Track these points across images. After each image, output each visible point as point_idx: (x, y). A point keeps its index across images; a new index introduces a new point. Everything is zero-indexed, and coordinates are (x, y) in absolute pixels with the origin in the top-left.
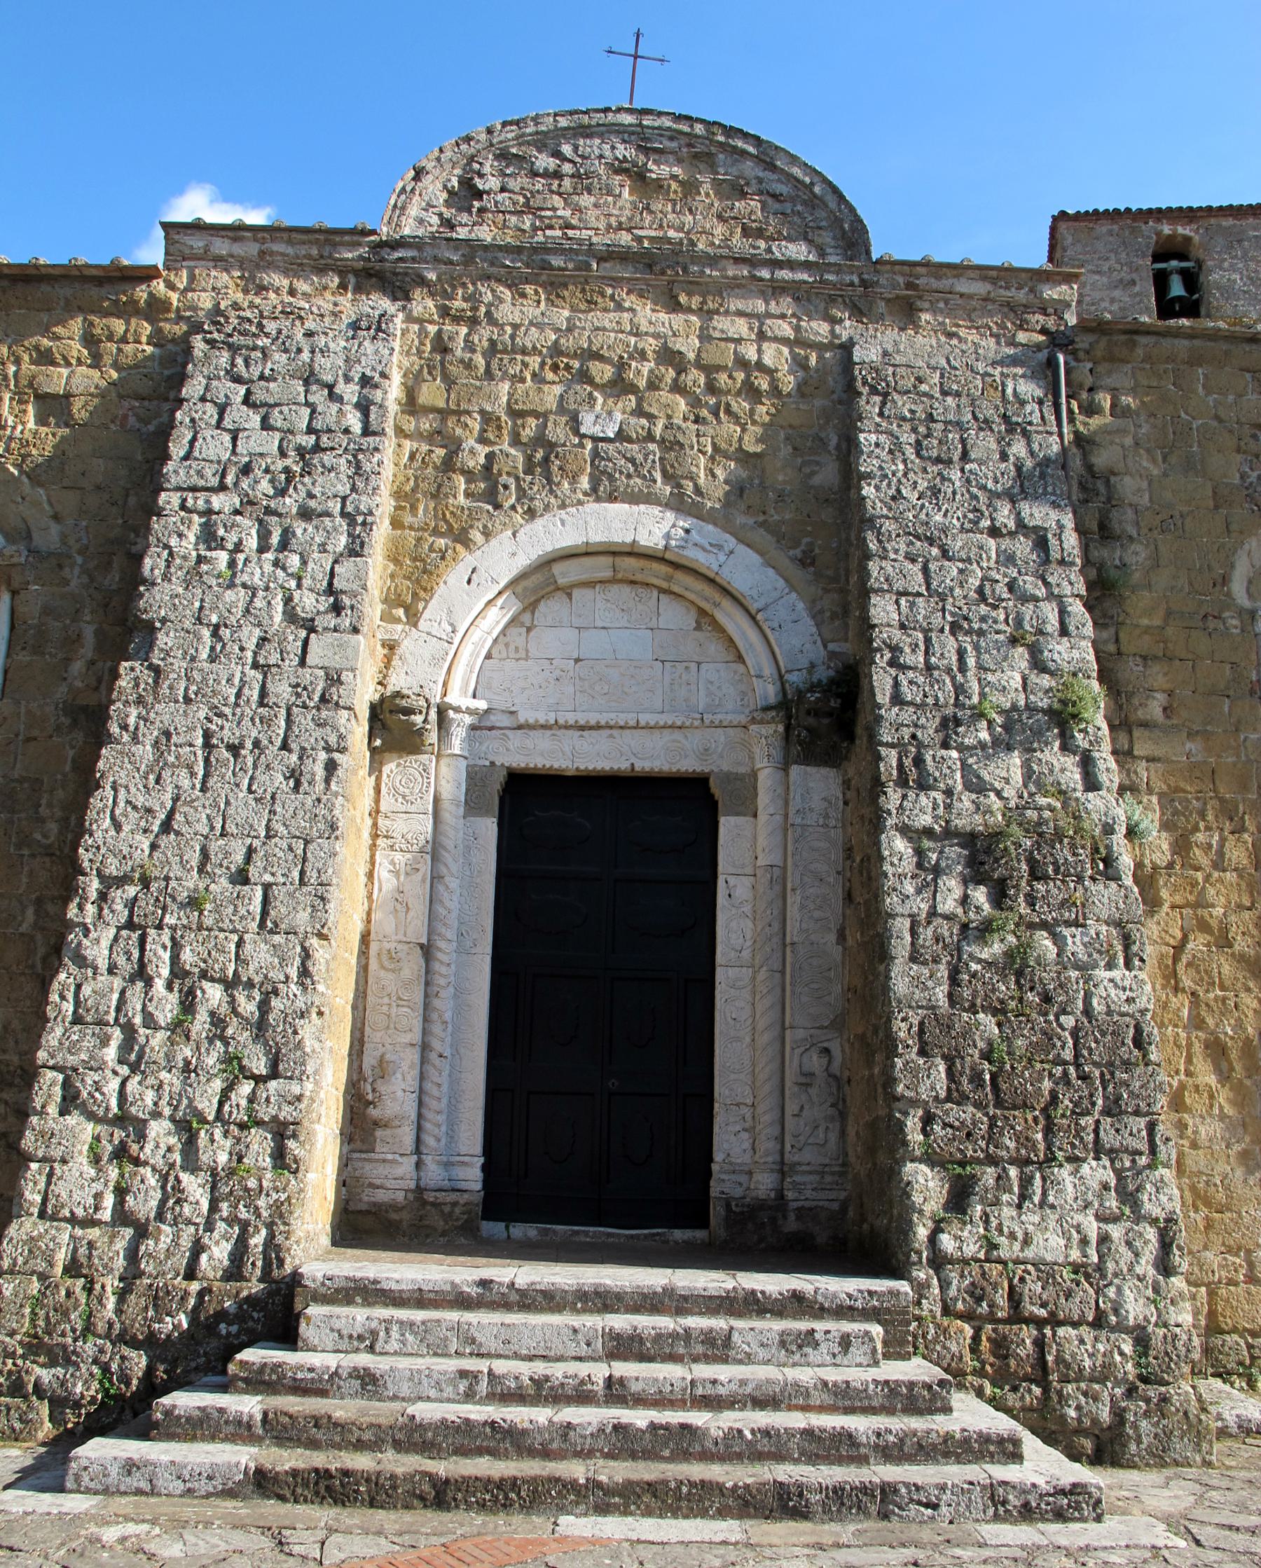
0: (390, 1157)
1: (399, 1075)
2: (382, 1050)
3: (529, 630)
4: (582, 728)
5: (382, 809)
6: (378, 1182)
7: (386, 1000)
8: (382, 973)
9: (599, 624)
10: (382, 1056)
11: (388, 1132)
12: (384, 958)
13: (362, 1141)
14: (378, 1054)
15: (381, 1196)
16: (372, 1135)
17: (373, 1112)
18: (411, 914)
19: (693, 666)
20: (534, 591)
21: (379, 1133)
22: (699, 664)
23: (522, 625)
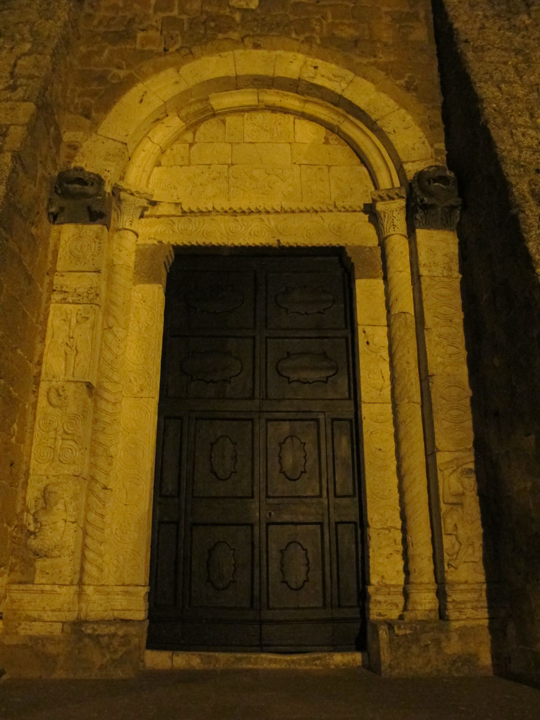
0: (48, 588)
1: (60, 506)
2: (46, 482)
3: (191, 145)
4: (235, 213)
5: (58, 269)
6: (35, 614)
7: (52, 434)
8: (50, 409)
9: (248, 140)
10: (45, 489)
11: (48, 561)
12: (53, 395)
13: (22, 572)
14: (41, 486)
15: (38, 629)
16: (32, 566)
17: (34, 543)
18: (81, 356)
19: (326, 170)
20: (195, 114)
21: (39, 564)
22: (329, 167)
23: (185, 142)
